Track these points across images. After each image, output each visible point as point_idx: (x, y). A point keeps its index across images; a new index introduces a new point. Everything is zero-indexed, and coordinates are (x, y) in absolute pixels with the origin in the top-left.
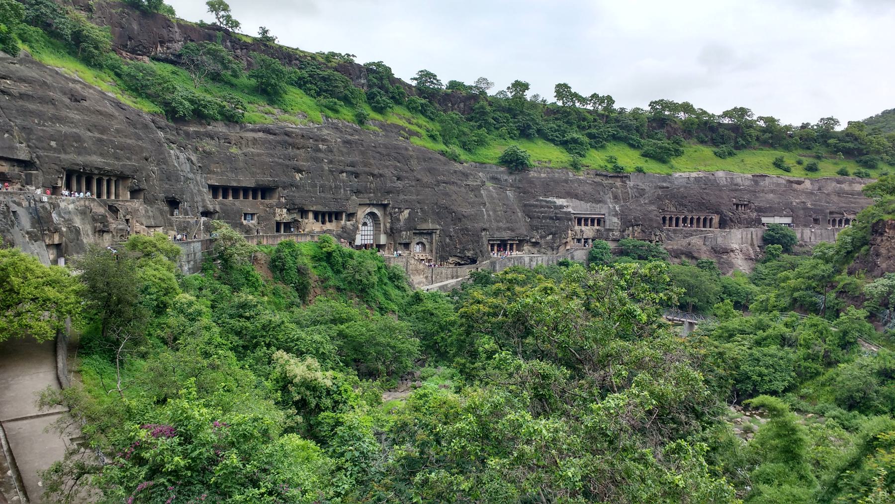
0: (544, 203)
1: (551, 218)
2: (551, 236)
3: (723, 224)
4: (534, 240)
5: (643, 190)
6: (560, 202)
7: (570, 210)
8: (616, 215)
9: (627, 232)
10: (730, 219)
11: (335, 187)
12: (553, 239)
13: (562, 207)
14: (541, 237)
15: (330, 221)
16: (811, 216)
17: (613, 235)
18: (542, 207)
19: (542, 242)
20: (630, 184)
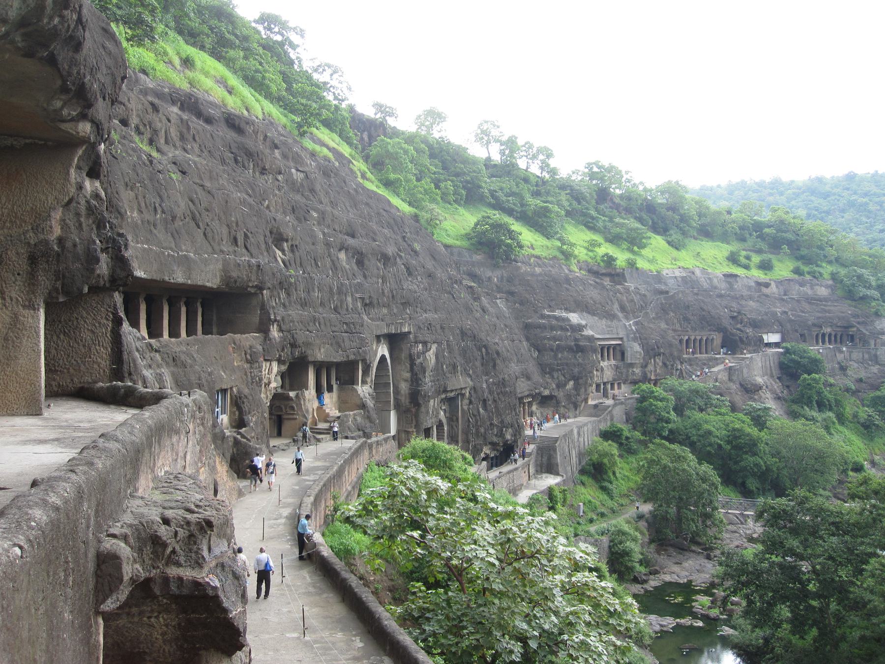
0: (554, 322)
1: (570, 349)
2: (571, 383)
3: (732, 344)
4: (546, 393)
5: (645, 295)
6: (574, 318)
7: (588, 332)
8: (635, 339)
9: (650, 367)
10: (740, 338)
11: (340, 292)
12: (577, 387)
13: (579, 328)
14: (560, 386)
15: (330, 389)
16: (796, 331)
17: (633, 373)
18: (552, 328)
19: (560, 394)
20: (631, 285)
